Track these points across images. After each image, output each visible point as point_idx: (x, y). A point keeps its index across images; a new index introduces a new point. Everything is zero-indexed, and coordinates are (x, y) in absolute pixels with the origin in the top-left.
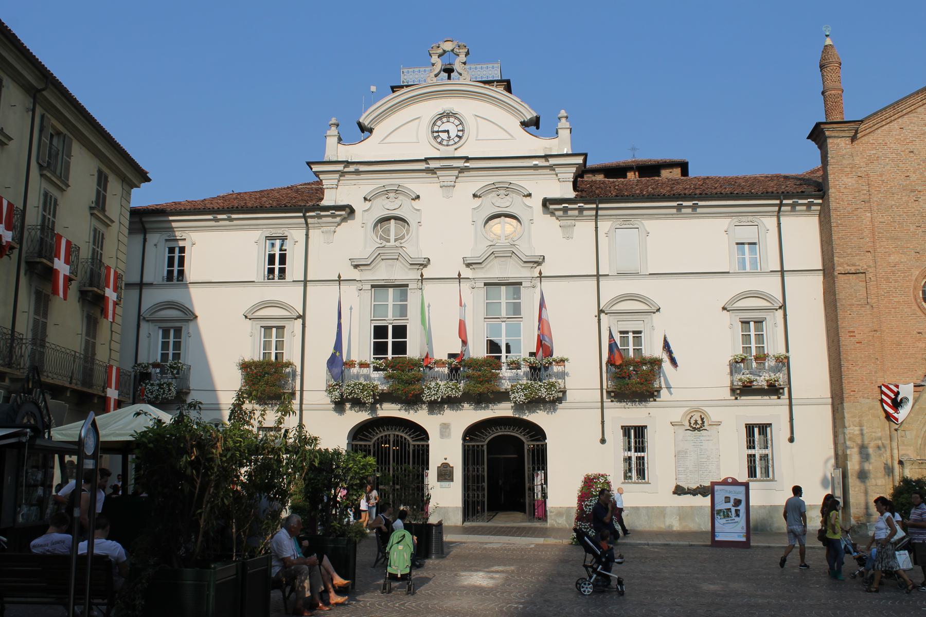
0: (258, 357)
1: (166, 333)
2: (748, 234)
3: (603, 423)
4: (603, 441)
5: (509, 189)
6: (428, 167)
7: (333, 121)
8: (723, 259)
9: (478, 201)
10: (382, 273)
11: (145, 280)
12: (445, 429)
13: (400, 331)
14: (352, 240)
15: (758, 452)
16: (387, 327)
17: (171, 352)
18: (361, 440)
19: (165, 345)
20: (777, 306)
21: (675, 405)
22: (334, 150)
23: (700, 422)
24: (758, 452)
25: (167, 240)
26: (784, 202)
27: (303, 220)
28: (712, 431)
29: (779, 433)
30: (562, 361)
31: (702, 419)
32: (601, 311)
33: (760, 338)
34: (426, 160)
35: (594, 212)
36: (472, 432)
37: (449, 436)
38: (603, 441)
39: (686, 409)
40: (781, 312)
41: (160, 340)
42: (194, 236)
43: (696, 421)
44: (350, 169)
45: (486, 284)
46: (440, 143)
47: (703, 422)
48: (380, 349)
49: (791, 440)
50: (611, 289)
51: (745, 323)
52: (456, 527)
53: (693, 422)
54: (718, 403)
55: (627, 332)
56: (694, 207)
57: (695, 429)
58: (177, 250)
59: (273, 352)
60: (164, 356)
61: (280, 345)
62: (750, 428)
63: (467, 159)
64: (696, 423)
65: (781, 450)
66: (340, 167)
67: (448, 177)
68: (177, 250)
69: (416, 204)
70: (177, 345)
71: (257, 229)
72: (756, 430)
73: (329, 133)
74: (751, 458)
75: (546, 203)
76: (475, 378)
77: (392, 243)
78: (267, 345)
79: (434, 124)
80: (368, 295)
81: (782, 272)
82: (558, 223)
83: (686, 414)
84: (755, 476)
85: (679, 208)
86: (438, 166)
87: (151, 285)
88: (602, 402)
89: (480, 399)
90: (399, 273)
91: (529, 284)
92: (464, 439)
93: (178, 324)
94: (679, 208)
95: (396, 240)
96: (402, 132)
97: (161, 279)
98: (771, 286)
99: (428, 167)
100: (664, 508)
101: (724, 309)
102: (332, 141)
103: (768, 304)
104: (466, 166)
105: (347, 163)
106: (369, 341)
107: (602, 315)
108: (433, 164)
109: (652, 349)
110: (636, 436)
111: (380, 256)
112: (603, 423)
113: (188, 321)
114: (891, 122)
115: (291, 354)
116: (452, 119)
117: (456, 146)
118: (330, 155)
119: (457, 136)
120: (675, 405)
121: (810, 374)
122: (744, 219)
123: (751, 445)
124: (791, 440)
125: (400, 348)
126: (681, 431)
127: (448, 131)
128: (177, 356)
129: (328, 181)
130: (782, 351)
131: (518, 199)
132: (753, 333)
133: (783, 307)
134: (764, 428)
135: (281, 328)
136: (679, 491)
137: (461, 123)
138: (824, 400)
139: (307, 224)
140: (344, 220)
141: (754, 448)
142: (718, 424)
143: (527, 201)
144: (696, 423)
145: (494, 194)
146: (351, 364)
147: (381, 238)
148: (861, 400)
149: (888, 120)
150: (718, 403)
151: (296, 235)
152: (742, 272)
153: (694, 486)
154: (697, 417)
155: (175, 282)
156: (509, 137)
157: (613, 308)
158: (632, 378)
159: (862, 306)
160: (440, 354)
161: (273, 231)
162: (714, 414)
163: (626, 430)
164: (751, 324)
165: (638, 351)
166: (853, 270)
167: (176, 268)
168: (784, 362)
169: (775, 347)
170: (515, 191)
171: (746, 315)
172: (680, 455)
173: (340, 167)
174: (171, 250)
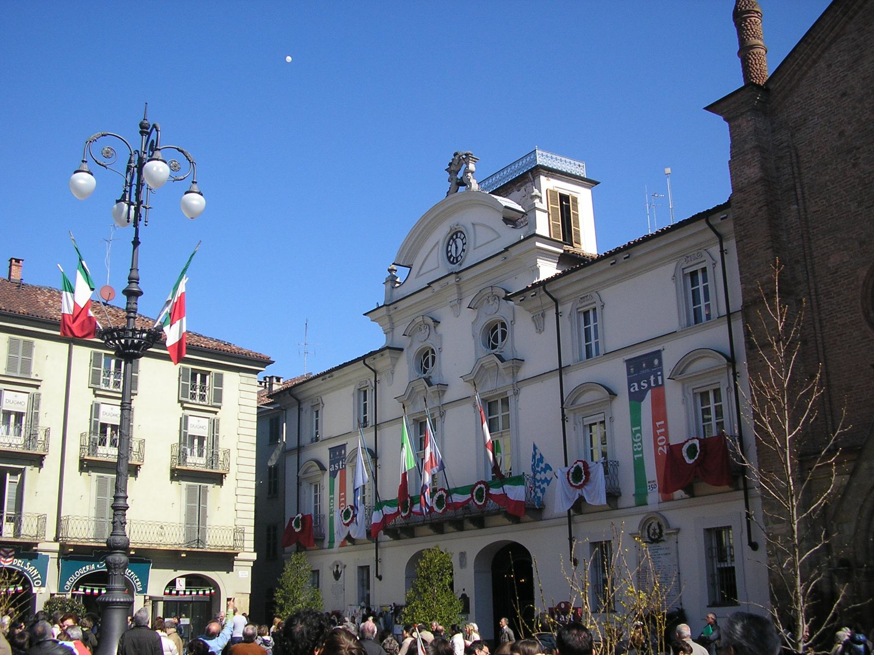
11: (302, 443)
23: (657, 531)
31: (660, 526)
34: (429, 285)
39: (642, 516)
43: (654, 530)
47: (661, 531)
50: (574, 379)
53: (651, 531)
57: (653, 541)
64: (654, 534)
79: (448, 244)
97: (309, 440)
114: (815, 62)
142: (678, 530)
144: (654, 530)
149: (809, 62)
154: (655, 525)
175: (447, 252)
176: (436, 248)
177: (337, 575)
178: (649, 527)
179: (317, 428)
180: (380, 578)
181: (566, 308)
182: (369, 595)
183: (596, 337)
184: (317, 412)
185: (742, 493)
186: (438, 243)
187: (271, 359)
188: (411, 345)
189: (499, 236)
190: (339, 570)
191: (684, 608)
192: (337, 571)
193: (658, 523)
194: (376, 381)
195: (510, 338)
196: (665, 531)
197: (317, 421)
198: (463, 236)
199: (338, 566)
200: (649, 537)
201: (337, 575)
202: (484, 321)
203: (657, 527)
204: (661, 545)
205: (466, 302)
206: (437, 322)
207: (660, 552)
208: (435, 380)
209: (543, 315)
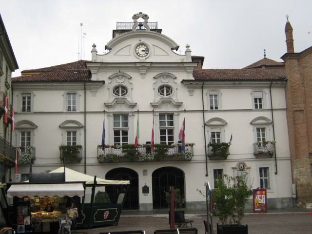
0: (66, 144)
1: (23, 134)
2: (258, 95)
3: (207, 168)
4: (207, 175)
5: (168, 76)
6: (135, 67)
8: (251, 105)
9: (155, 81)
10: (119, 109)
13: (125, 133)
14: (105, 96)
16: (119, 131)
17: (26, 142)
19: (23, 139)
21: (233, 161)
24: (263, 178)
25: (22, 94)
28: (247, 171)
29: (271, 172)
30: (192, 145)
34: (135, 63)
37: (146, 175)
38: (207, 175)
40: (271, 127)
41: (21, 137)
42: (35, 92)
46: (139, 56)
47: (244, 167)
48: (117, 140)
49: (276, 173)
51: (258, 130)
52: (151, 211)
54: (249, 160)
55: (214, 133)
57: (241, 170)
58: (27, 98)
59: (72, 141)
60: (23, 144)
61: (74, 139)
62: (261, 169)
63: (152, 63)
64: (241, 167)
65: (272, 178)
66: (99, 65)
67: (143, 71)
68: (27, 98)
69: (131, 81)
70: (29, 139)
74: (261, 180)
75: (183, 81)
76: (158, 151)
77: (120, 97)
78: (69, 139)
80: (112, 119)
81: (272, 110)
86: (140, 65)
87: (16, 113)
88: (206, 160)
89: (157, 159)
90: (124, 109)
91: (177, 114)
92: (152, 176)
93: (29, 130)
95: (122, 95)
98: (268, 115)
104: (151, 66)
105: (102, 63)
106: (113, 136)
109: (225, 139)
111: (117, 102)
112: (207, 168)
113: (34, 129)
115: (80, 141)
116: (143, 46)
117: (146, 57)
120: (233, 161)
121: (283, 148)
122: (257, 89)
123: (261, 176)
124: (276, 173)
125: (125, 139)
127: (142, 51)
128: (29, 144)
130: (272, 140)
131: (171, 80)
132: (261, 133)
134: (266, 169)
135: (75, 133)
137: (147, 48)
139: (85, 88)
140: (101, 86)
142: (249, 168)
143: (175, 81)
144: (241, 167)
146: (108, 147)
147: (116, 94)
148: (303, 158)
150: (249, 160)
151: (81, 93)
154: (242, 165)
155: (26, 112)
156: (166, 54)
158: (218, 151)
159: (303, 123)
160: (142, 142)
162: (248, 164)
163: (215, 171)
164: (260, 130)
165: (219, 140)
166: (299, 109)
167: (26, 106)
168: (273, 144)
169: (269, 138)
170: (171, 77)
171: (258, 126)
173: (99, 65)
174: (24, 98)
175: (136, 51)
176: (129, 47)
181: (205, 91)
189: (168, 55)
202: (160, 84)
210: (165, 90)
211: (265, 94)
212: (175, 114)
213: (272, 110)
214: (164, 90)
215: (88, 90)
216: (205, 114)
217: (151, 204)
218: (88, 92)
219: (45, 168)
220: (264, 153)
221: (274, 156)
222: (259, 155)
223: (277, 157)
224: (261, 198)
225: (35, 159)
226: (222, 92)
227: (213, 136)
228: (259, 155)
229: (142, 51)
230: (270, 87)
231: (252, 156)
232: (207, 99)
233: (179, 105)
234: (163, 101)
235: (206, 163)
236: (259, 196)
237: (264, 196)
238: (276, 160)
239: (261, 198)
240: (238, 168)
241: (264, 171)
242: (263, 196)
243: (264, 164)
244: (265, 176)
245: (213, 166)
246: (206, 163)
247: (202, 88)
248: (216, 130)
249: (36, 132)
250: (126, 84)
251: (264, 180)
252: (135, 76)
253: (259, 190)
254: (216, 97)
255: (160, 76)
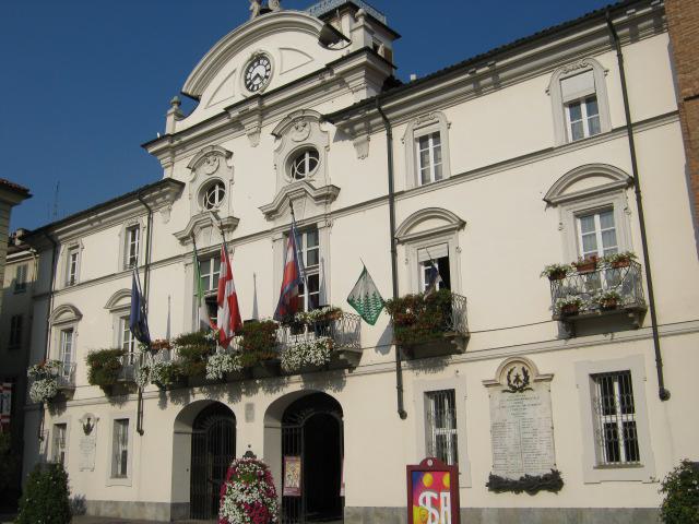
2: (578, 86)
4: (403, 415)
5: (306, 118)
6: (234, 119)
7: (176, 99)
9: (279, 142)
12: (250, 407)
15: (619, 419)
18: (201, 428)
20: (623, 181)
22: (173, 125)
23: (522, 377)
24: (619, 419)
25: (71, 249)
26: (614, 22)
27: (143, 206)
31: (525, 373)
32: (395, 242)
33: (609, 235)
34: (228, 110)
35: (381, 119)
36: (271, 411)
38: (403, 415)
39: (501, 361)
43: (517, 377)
44: (179, 142)
45: (287, 234)
47: (527, 378)
49: (664, 395)
50: (405, 209)
53: (513, 378)
56: (495, 73)
57: (515, 390)
63: (261, 97)
64: (517, 380)
71: (121, 222)
72: (616, 386)
73: (169, 112)
79: (247, 72)
82: (352, 142)
83: (502, 369)
84: (618, 459)
85: (476, 80)
87: (57, 292)
93: (70, 326)
94: (476, 80)
96: (222, 88)
98: (613, 153)
99: (234, 119)
100: (479, 511)
101: (550, 203)
102: (170, 119)
103: (609, 181)
107: (400, 249)
108: (235, 114)
110: (443, 402)
118: (169, 131)
119: (267, 77)
122: (570, 66)
124: (664, 395)
126: (497, 392)
127: (258, 75)
129: (165, 160)
133: (633, 182)
134: (625, 378)
136: (497, 484)
138: (690, 326)
141: (613, 412)
142: (550, 378)
144: (517, 377)
145: (293, 129)
152: (578, 140)
153: (516, 477)
154: (518, 370)
157: (411, 232)
158: (429, 328)
161: (130, 221)
162: (542, 364)
170: (311, 119)
172: (497, 429)
173: (166, 144)
176: (232, 77)
177: (88, 430)
178: (509, 373)
179: (73, 271)
180: (141, 432)
181: (399, 131)
182: (125, 453)
183: (437, 159)
184: (74, 256)
185: (650, 331)
186: (234, 71)
187: (30, 193)
188: (192, 181)
190: (91, 423)
191: (559, 468)
192: (88, 425)
193: (523, 369)
194: (149, 218)
195: (322, 167)
196: (530, 380)
197: (74, 265)
198: (266, 62)
199: (89, 419)
200: (509, 385)
201: (88, 430)
203: (521, 373)
204: (527, 394)
205: (267, 130)
206: (229, 155)
207: (525, 402)
208: (223, 214)
209: (369, 140)
210: (303, 159)
211: (600, 73)
212: (319, 226)
213: (630, 128)
214: (304, 163)
215: (157, 210)
216: (400, 205)
217: (403, 509)
218: (157, 216)
219: (84, 407)
220: (600, 306)
221: (648, 320)
222: (573, 321)
223: (659, 322)
224: (436, 503)
225: (73, 391)
226: (449, 120)
227: (430, 275)
228: (573, 321)
229: (258, 75)
230: (616, 44)
231: (554, 329)
232: (404, 153)
233: (330, 194)
234: (286, 196)
235: (399, 371)
236: (429, 495)
237: (448, 495)
238: (656, 337)
239: (436, 503)
240: (505, 381)
241: (614, 388)
242: (445, 495)
243: (608, 352)
244: (623, 412)
245: (420, 381)
246: (399, 371)
247: (388, 125)
248: (437, 252)
249: (80, 327)
250: (223, 175)
251: (620, 425)
252: (234, 143)
253: (430, 470)
254: (439, 142)
255: (286, 129)
